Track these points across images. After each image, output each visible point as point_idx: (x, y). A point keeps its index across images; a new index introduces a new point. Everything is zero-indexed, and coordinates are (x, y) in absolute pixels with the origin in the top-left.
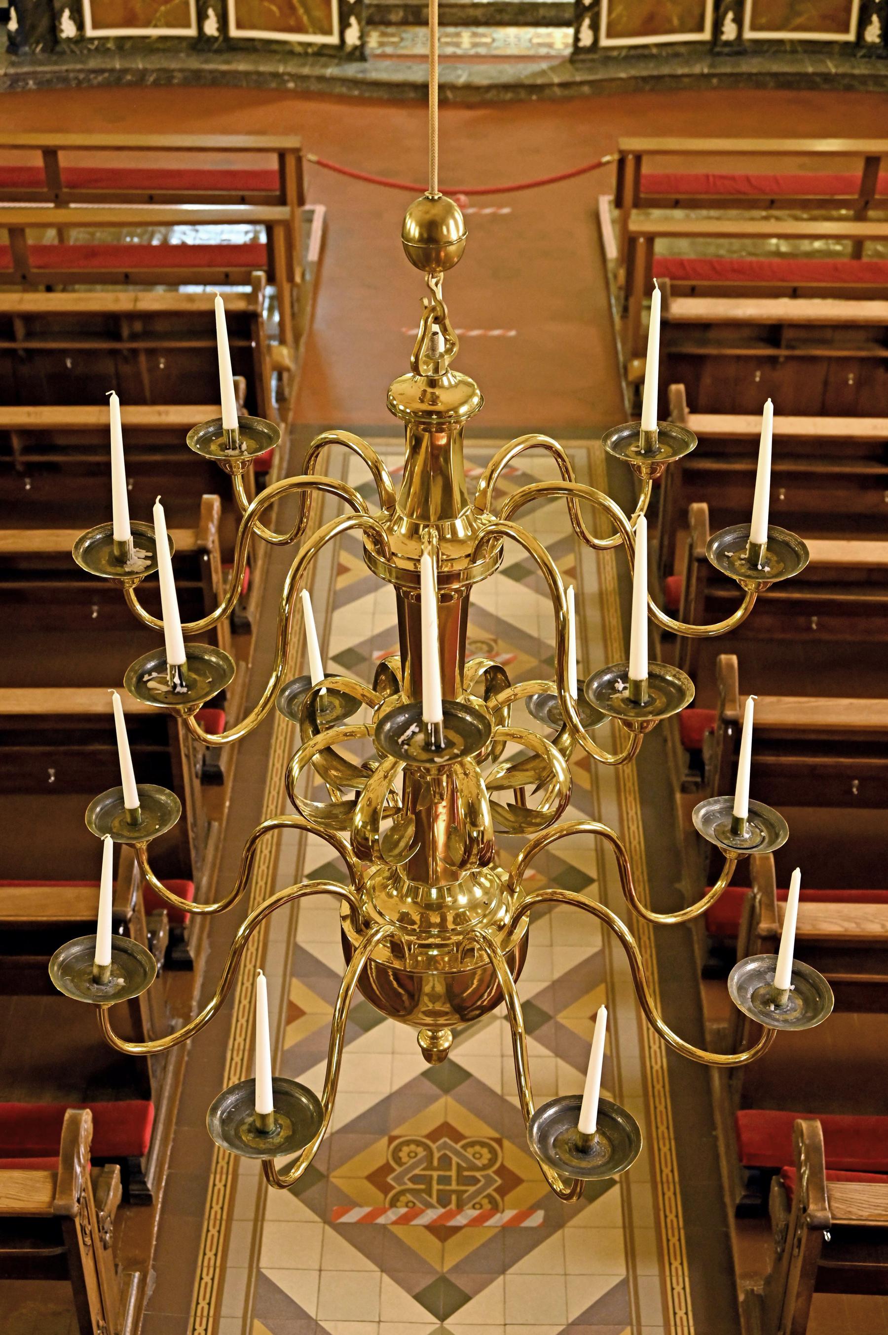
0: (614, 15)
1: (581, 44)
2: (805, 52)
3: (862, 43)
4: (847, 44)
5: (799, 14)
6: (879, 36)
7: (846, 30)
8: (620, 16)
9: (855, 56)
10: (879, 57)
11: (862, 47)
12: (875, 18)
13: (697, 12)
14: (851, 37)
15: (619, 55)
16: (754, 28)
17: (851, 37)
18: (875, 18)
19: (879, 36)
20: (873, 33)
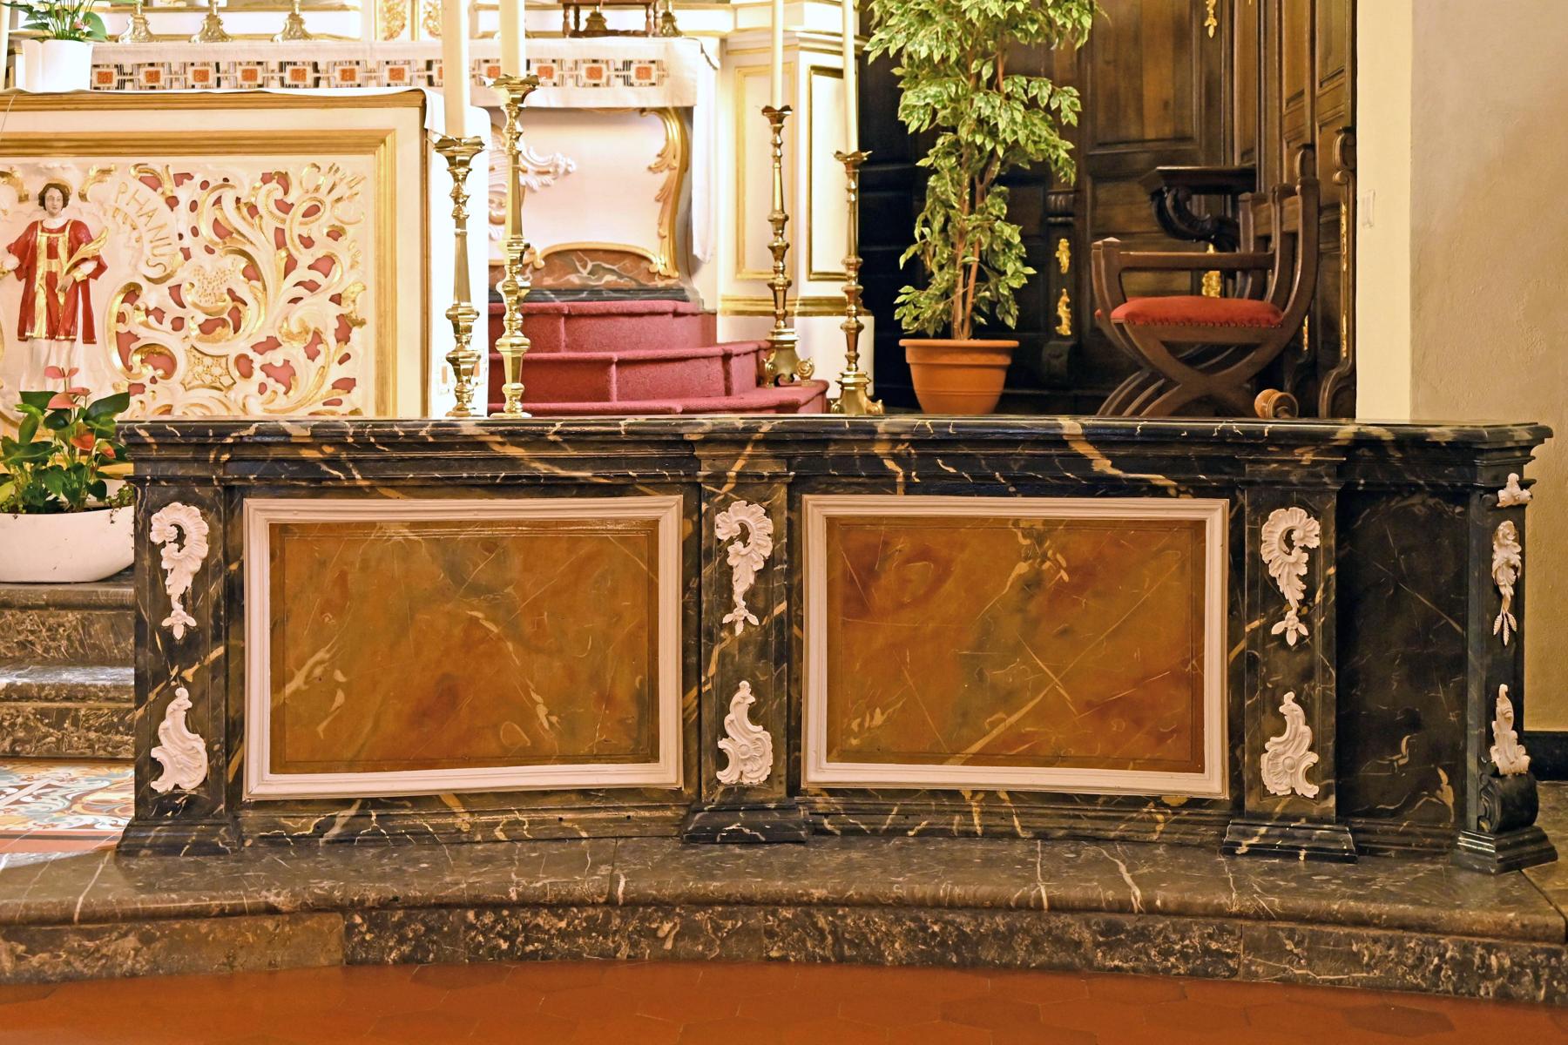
0: (296, 683)
1: (161, 786)
2: (1043, 836)
3: (1250, 803)
5: (1008, 699)
8: (322, 687)
9: (1230, 850)
10: (1319, 855)
11: (1263, 817)
12: (1289, 706)
13: (625, 684)
14: (1212, 782)
15: (321, 829)
16: (837, 750)
17: (1212, 782)
18: (1289, 706)
19: (1310, 775)
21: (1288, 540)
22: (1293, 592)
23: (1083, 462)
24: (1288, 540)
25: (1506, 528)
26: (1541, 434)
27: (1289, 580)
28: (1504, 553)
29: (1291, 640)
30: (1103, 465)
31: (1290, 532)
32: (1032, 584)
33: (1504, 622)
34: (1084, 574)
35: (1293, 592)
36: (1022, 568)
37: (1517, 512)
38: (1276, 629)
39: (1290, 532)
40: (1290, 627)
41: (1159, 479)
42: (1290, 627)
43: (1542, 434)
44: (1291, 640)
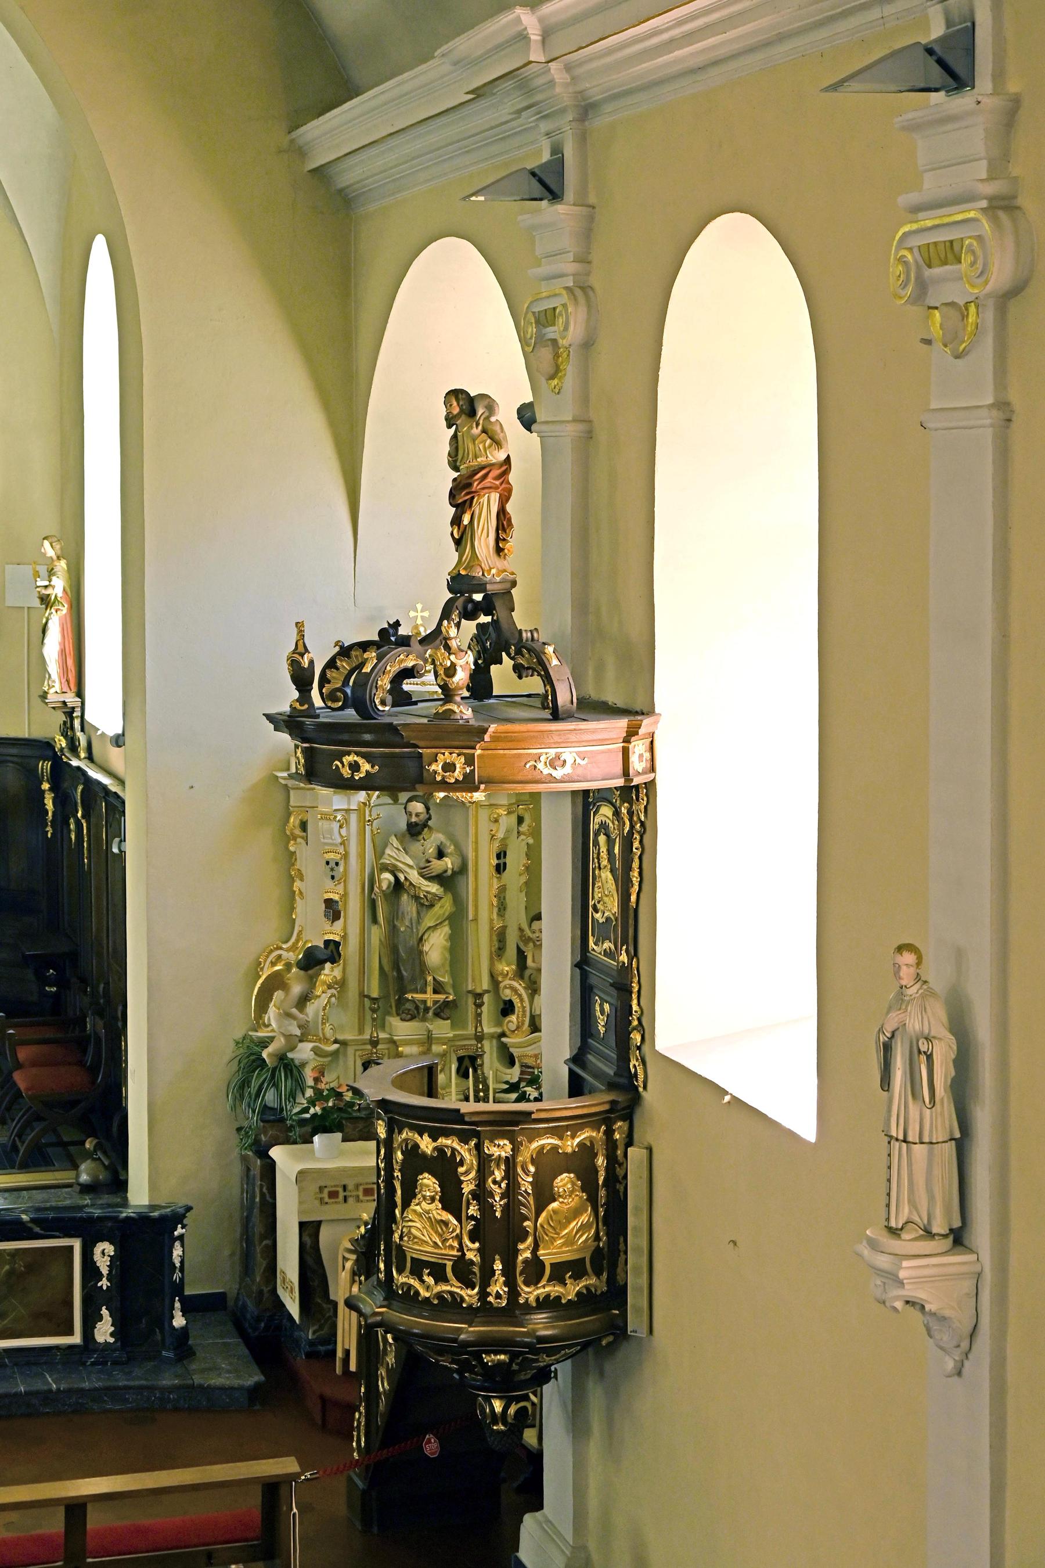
3: (91, 1347)
4: (71, 1347)
6: (112, 1335)
7: (70, 1332)
10: (115, 1363)
12: (104, 1312)
18: (104, 1312)
19: (112, 1335)
20: (104, 1331)
21: (103, 1253)
22: (105, 1271)
23: (31, 1229)
24: (103, 1253)
25: (177, 1244)
26: (189, 1209)
27: (103, 1264)
28: (177, 1252)
29: (105, 1288)
30: (37, 1229)
31: (104, 1250)
32: (11, 1273)
33: (177, 1276)
34: (30, 1268)
35: (105, 1271)
36: (7, 1267)
37: (181, 1238)
38: (99, 1284)
39: (104, 1250)
40: (104, 1283)
41: (57, 1234)
42: (104, 1283)
43: (189, 1209)
44: (105, 1288)
